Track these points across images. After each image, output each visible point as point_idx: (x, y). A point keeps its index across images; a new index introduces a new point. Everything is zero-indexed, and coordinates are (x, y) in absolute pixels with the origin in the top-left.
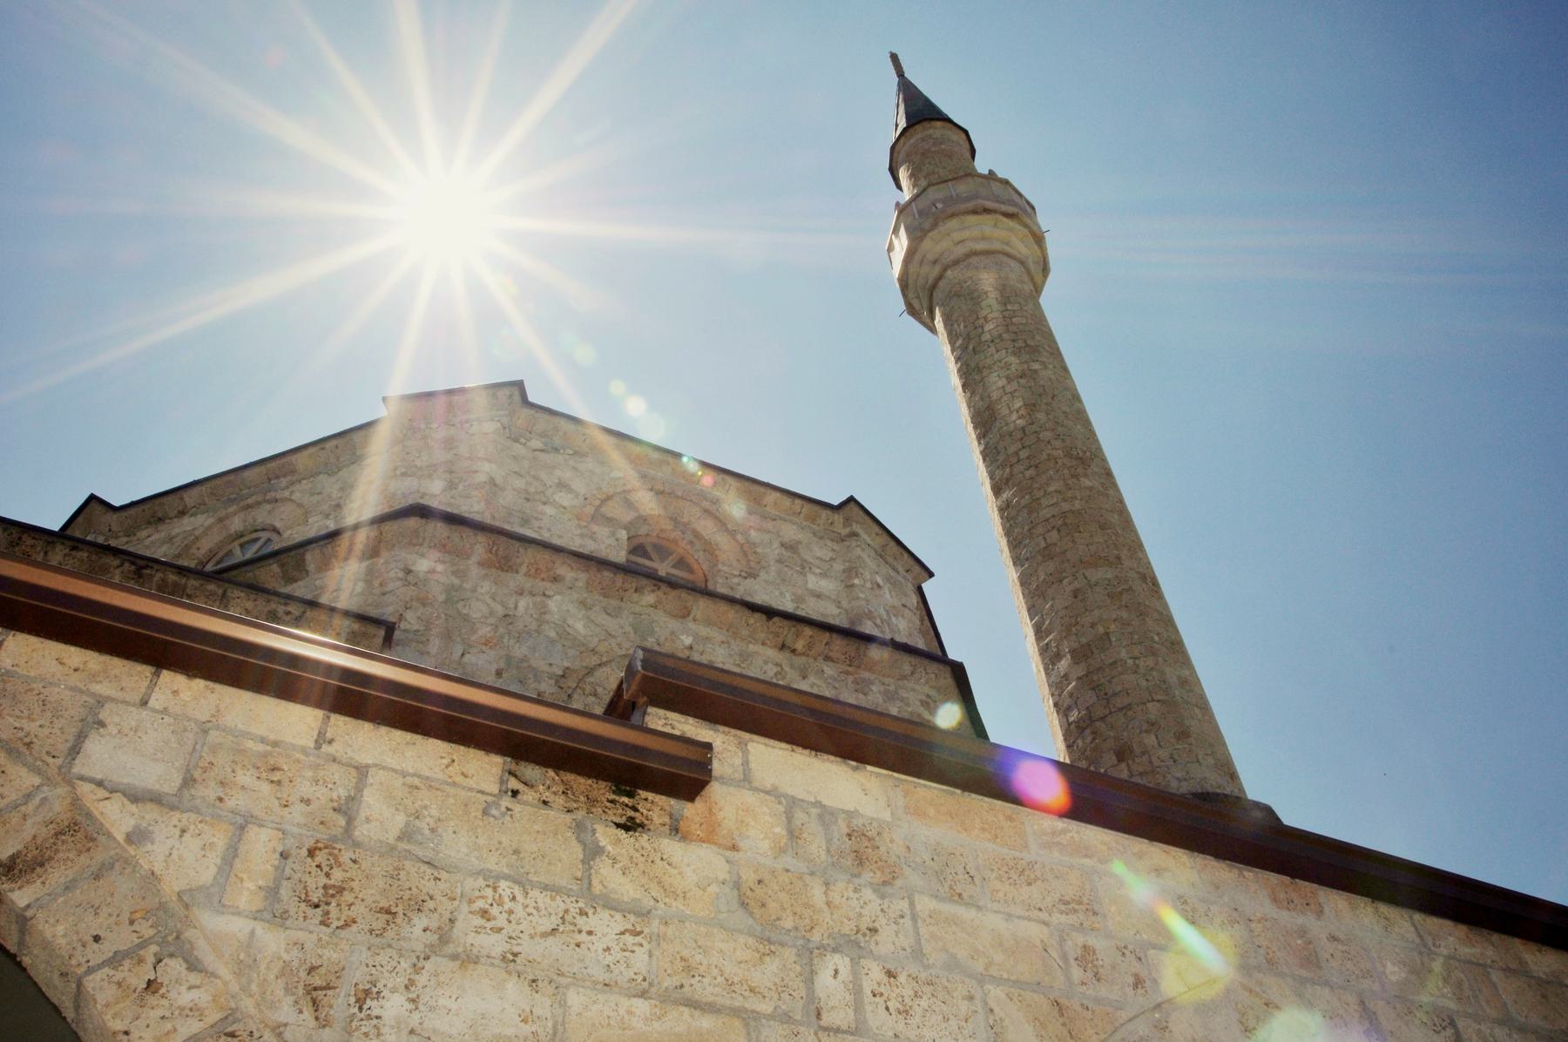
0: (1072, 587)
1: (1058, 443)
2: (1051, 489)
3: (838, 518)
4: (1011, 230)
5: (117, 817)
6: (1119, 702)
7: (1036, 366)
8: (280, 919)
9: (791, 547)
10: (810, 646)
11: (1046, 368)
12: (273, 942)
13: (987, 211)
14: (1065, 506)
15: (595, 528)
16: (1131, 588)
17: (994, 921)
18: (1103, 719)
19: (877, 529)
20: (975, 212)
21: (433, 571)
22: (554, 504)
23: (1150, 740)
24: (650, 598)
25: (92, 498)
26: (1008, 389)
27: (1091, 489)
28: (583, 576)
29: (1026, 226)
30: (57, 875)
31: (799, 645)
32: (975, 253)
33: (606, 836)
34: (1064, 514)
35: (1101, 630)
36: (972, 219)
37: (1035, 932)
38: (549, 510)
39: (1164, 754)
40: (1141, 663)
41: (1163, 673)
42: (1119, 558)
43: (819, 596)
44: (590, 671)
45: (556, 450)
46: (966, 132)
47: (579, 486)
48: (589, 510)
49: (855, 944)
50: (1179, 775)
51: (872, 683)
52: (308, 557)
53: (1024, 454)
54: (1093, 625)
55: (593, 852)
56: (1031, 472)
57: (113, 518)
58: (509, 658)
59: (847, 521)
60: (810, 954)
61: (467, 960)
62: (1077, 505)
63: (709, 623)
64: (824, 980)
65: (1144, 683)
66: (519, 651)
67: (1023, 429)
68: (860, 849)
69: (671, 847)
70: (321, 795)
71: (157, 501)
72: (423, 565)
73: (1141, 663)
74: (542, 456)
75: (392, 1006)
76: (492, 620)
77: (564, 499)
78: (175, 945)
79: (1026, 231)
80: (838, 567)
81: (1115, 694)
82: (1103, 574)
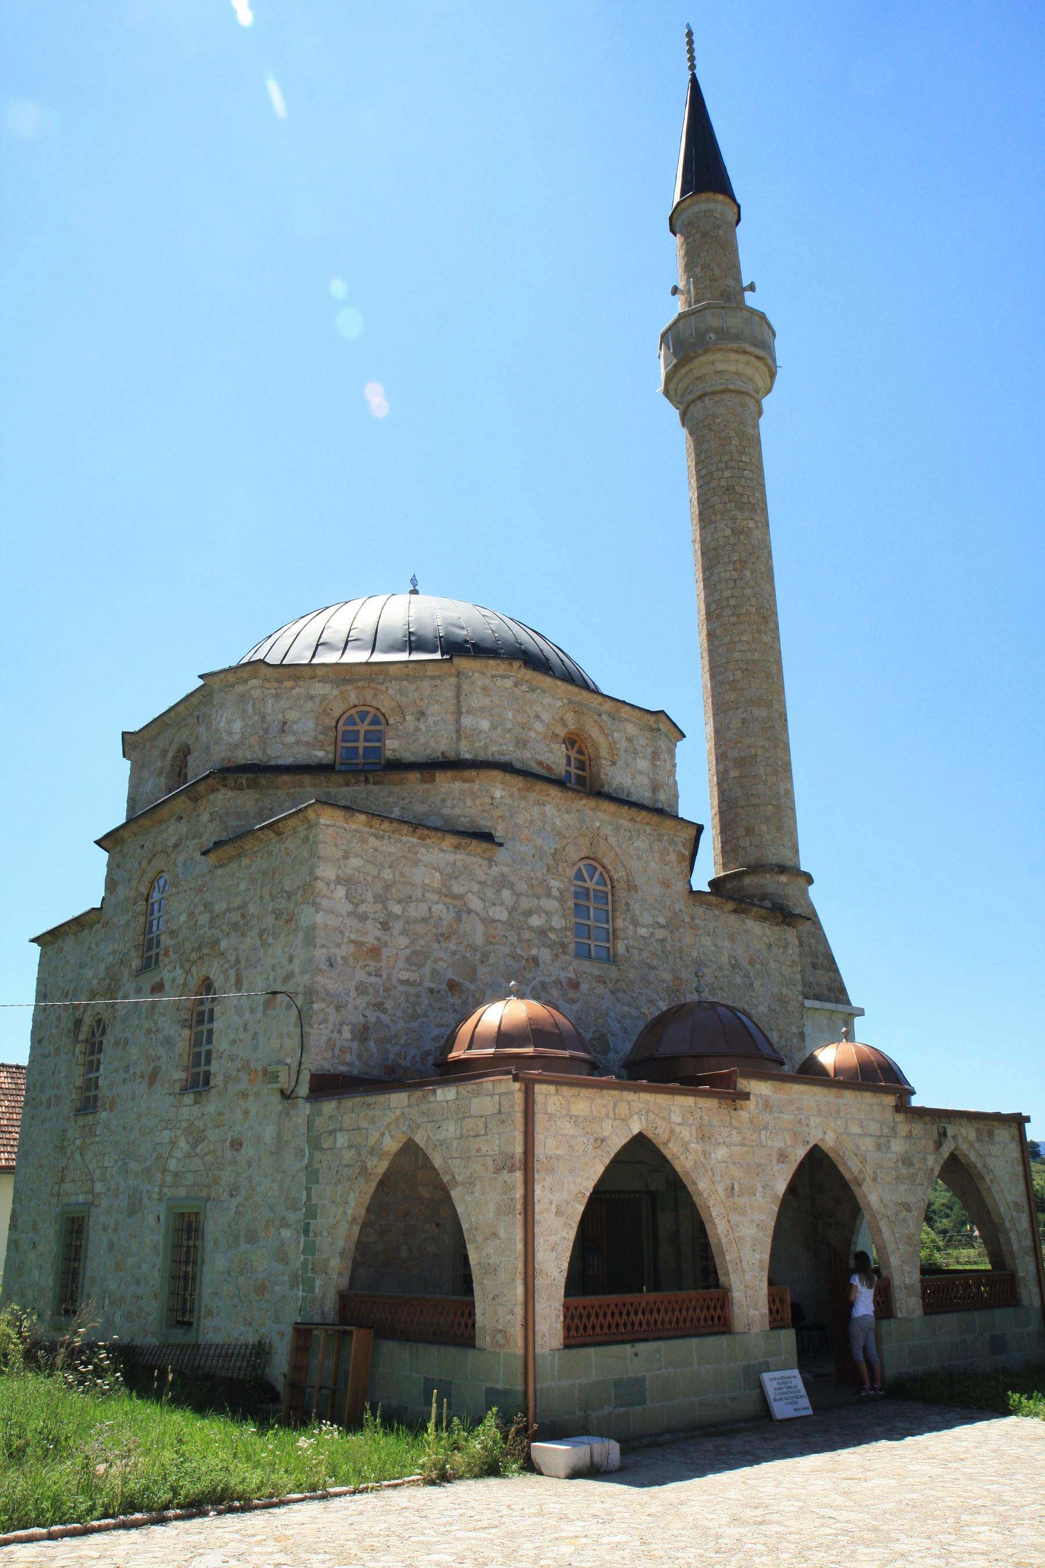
0: (742, 716)
1: (754, 601)
2: (744, 638)
3: (652, 719)
4: (757, 368)
5: (677, 1129)
6: (754, 800)
7: (751, 524)
8: (698, 1143)
9: (629, 740)
10: (642, 819)
11: (757, 527)
12: (699, 1147)
13: (745, 352)
14: (749, 656)
15: (553, 745)
16: (773, 727)
17: (786, 1116)
18: (743, 807)
19: (668, 722)
20: (737, 351)
21: (502, 797)
22: (535, 730)
23: (764, 828)
26: (732, 540)
27: (766, 644)
28: (560, 794)
29: (767, 366)
30: (673, 1140)
31: (638, 819)
32: (729, 391)
33: (733, 1113)
34: (747, 662)
35: (753, 752)
36: (733, 356)
37: (792, 1117)
38: (532, 734)
39: (769, 837)
40: (769, 778)
41: (778, 787)
42: (771, 702)
43: (640, 773)
44: (564, 848)
45: (533, 691)
46: (739, 207)
47: (545, 716)
48: (550, 733)
49: (765, 1128)
50: (774, 851)
51: (663, 835)
52: (437, 775)
53: (732, 602)
54: (749, 747)
55: (731, 1117)
56: (733, 619)
57: (269, 672)
58: (535, 846)
59: (657, 721)
60: (760, 1131)
61: (719, 1144)
62: (757, 656)
63: (604, 811)
64: (763, 1137)
65: (768, 792)
66: (539, 842)
67: (735, 580)
68: (767, 1105)
69: (741, 1112)
70: (698, 1116)
71: (299, 668)
72: (498, 794)
73: (769, 778)
74: (527, 694)
75: (713, 1155)
76: (527, 824)
77: (539, 727)
78: (687, 1150)
79: (766, 370)
80: (649, 750)
81: (752, 795)
82: (760, 712)
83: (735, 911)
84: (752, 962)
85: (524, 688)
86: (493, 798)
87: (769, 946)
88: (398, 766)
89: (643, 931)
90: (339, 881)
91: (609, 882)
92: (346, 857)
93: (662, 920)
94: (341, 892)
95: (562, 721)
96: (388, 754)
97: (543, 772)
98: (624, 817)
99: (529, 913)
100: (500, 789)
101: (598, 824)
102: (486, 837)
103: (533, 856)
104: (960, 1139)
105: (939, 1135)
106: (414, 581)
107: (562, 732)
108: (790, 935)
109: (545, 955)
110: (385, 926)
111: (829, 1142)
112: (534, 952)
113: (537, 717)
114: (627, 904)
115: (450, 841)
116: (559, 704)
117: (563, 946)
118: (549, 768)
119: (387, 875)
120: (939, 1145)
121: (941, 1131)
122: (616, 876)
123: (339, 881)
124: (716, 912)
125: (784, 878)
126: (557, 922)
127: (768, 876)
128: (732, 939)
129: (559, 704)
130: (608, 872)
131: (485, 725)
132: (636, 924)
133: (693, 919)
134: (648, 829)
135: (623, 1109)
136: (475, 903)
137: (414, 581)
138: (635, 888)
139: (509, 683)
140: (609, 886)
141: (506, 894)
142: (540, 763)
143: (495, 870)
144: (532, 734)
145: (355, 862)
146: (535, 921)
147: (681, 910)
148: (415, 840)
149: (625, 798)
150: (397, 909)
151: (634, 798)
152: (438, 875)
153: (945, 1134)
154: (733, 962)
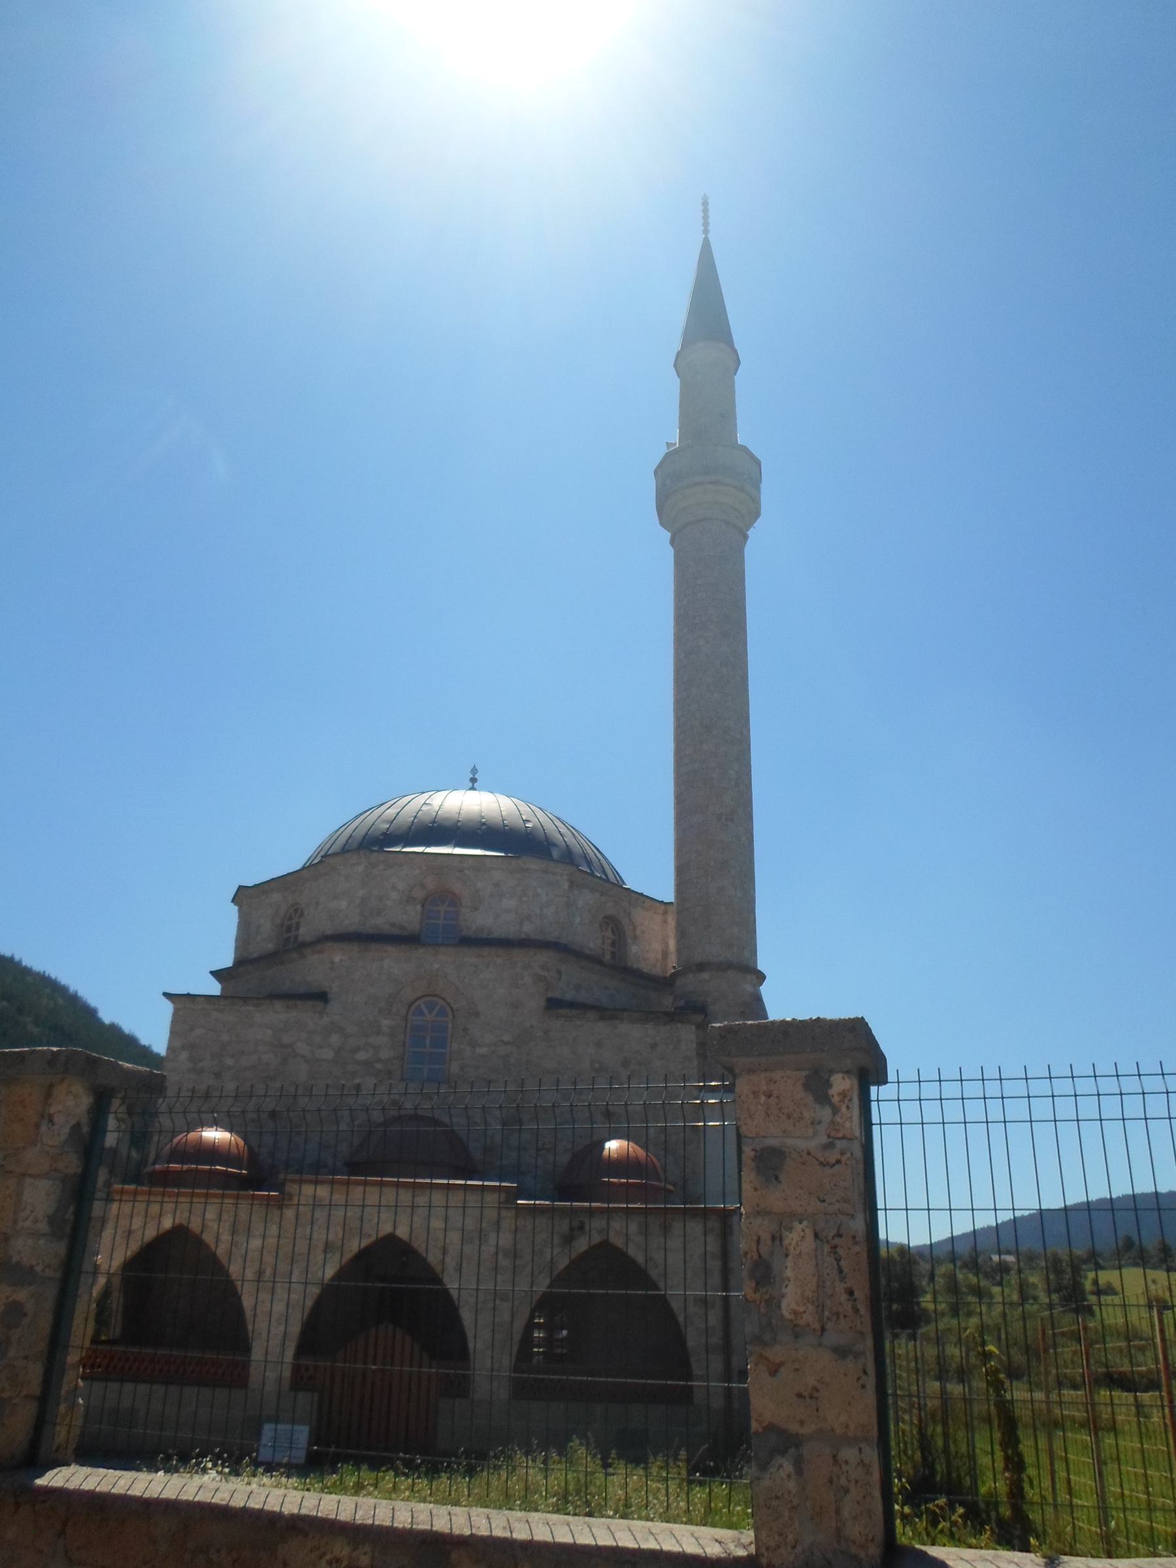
9: (497, 885)
21: (341, 960)
24: (421, 951)
25: (241, 888)
72: (337, 959)
83: (602, 1018)
84: (625, 1064)
85: (381, 867)
86: (333, 963)
87: (654, 1046)
88: (304, 945)
89: (483, 1050)
90: (183, 1047)
91: (450, 1013)
92: (192, 1029)
93: (507, 1038)
94: (184, 1055)
95: (423, 886)
96: (300, 939)
97: (396, 931)
98: (470, 957)
99: (357, 1049)
100: (339, 955)
101: (436, 966)
102: (321, 997)
103: (366, 1003)
104: (612, 1234)
105: (572, 1229)
106: (474, 771)
107: (419, 894)
108: (687, 1034)
109: (369, 1082)
110: (218, 1075)
111: (402, 1232)
112: (357, 1081)
113: (394, 887)
114: (465, 1030)
115: (279, 1005)
116: (417, 871)
117: (389, 1073)
118: (402, 927)
119: (225, 1037)
120: (568, 1239)
121: (576, 1224)
122: (455, 1007)
123: (183, 1047)
124: (578, 1022)
125: (705, 976)
126: (385, 1054)
127: (691, 975)
128: (599, 1045)
129: (417, 871)
130: (448, 1004)
131: (344, 904)
132: (474, 1044)
133: (546, 1032)
134: (499, 961)
135: (155, 1208)
136: (302, 1048)
137: (474, 771)
138: (477, 1014)
139: (361, 868)
140: (450, 1016)
141: (335, 1039)
142: (393, 925)
143: (326, 1020)
144: (389, 903)
145: (198, 1032)
146: (362, 1056)
147: (532, 1026)
148: (251, 1008)
149: (485, 936)
150: (229, 1062)
151: (496, 935)
152: (269, 1032)
153: (581, 1228)
154: (597, 1066)
